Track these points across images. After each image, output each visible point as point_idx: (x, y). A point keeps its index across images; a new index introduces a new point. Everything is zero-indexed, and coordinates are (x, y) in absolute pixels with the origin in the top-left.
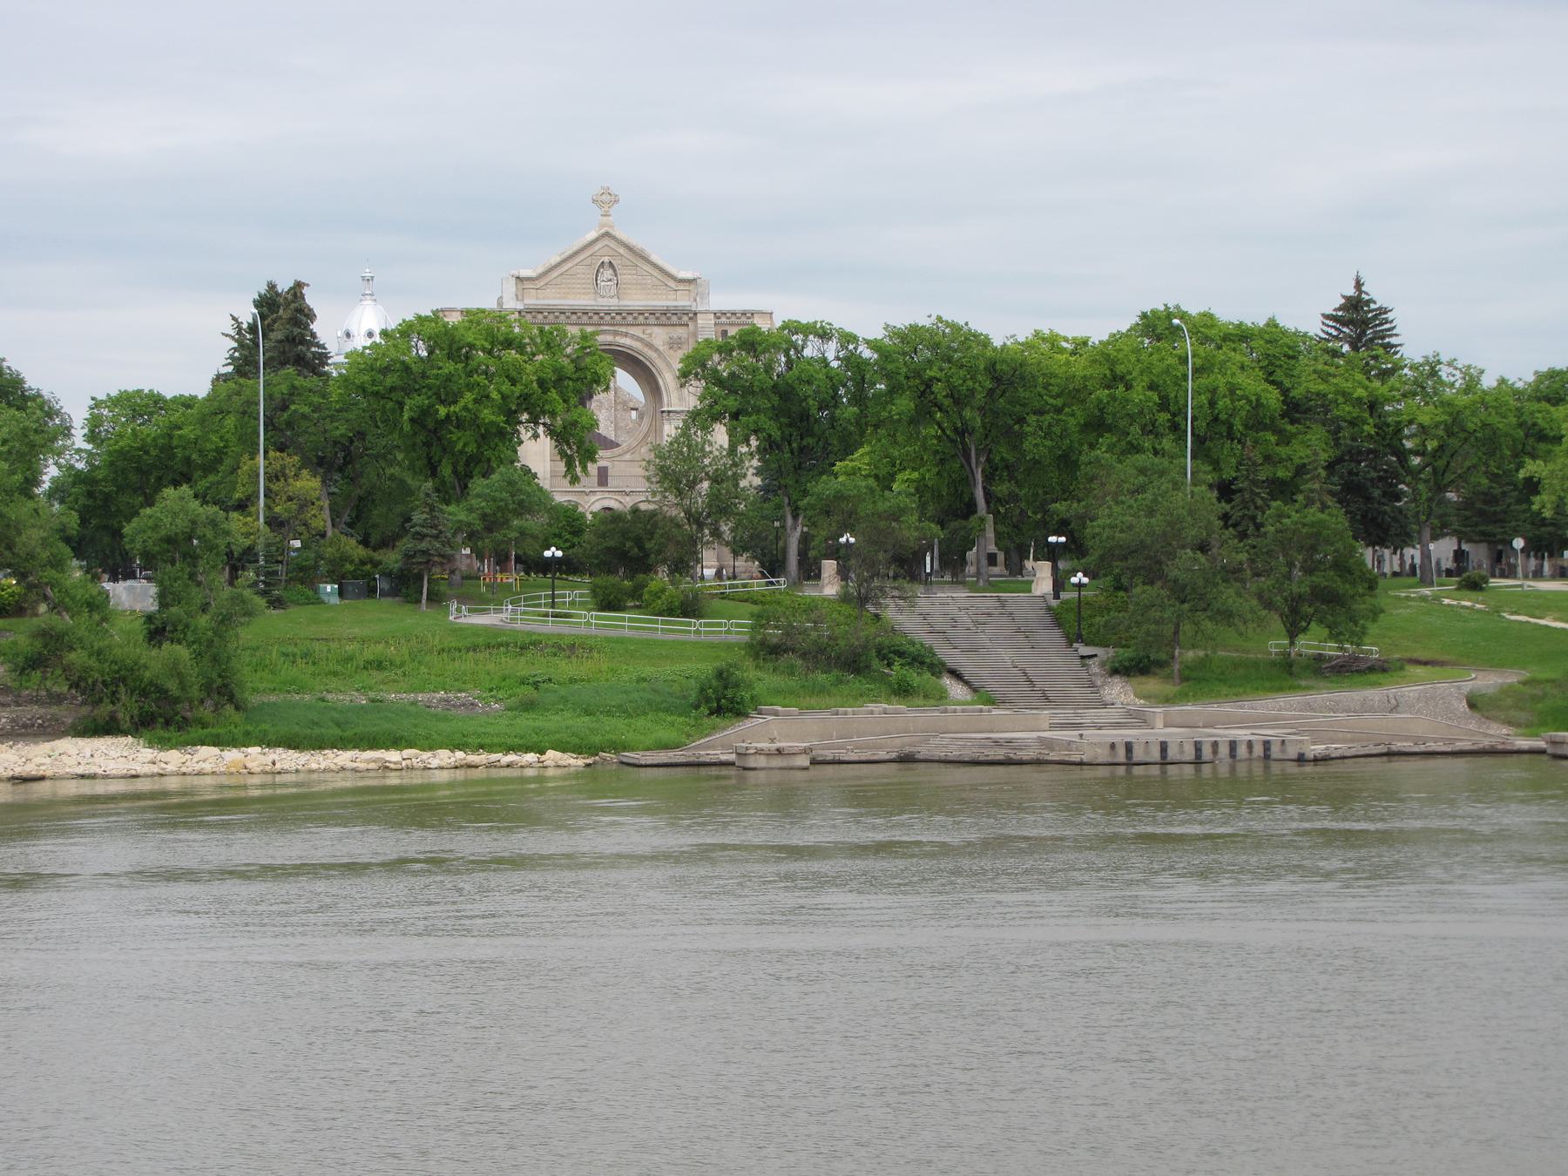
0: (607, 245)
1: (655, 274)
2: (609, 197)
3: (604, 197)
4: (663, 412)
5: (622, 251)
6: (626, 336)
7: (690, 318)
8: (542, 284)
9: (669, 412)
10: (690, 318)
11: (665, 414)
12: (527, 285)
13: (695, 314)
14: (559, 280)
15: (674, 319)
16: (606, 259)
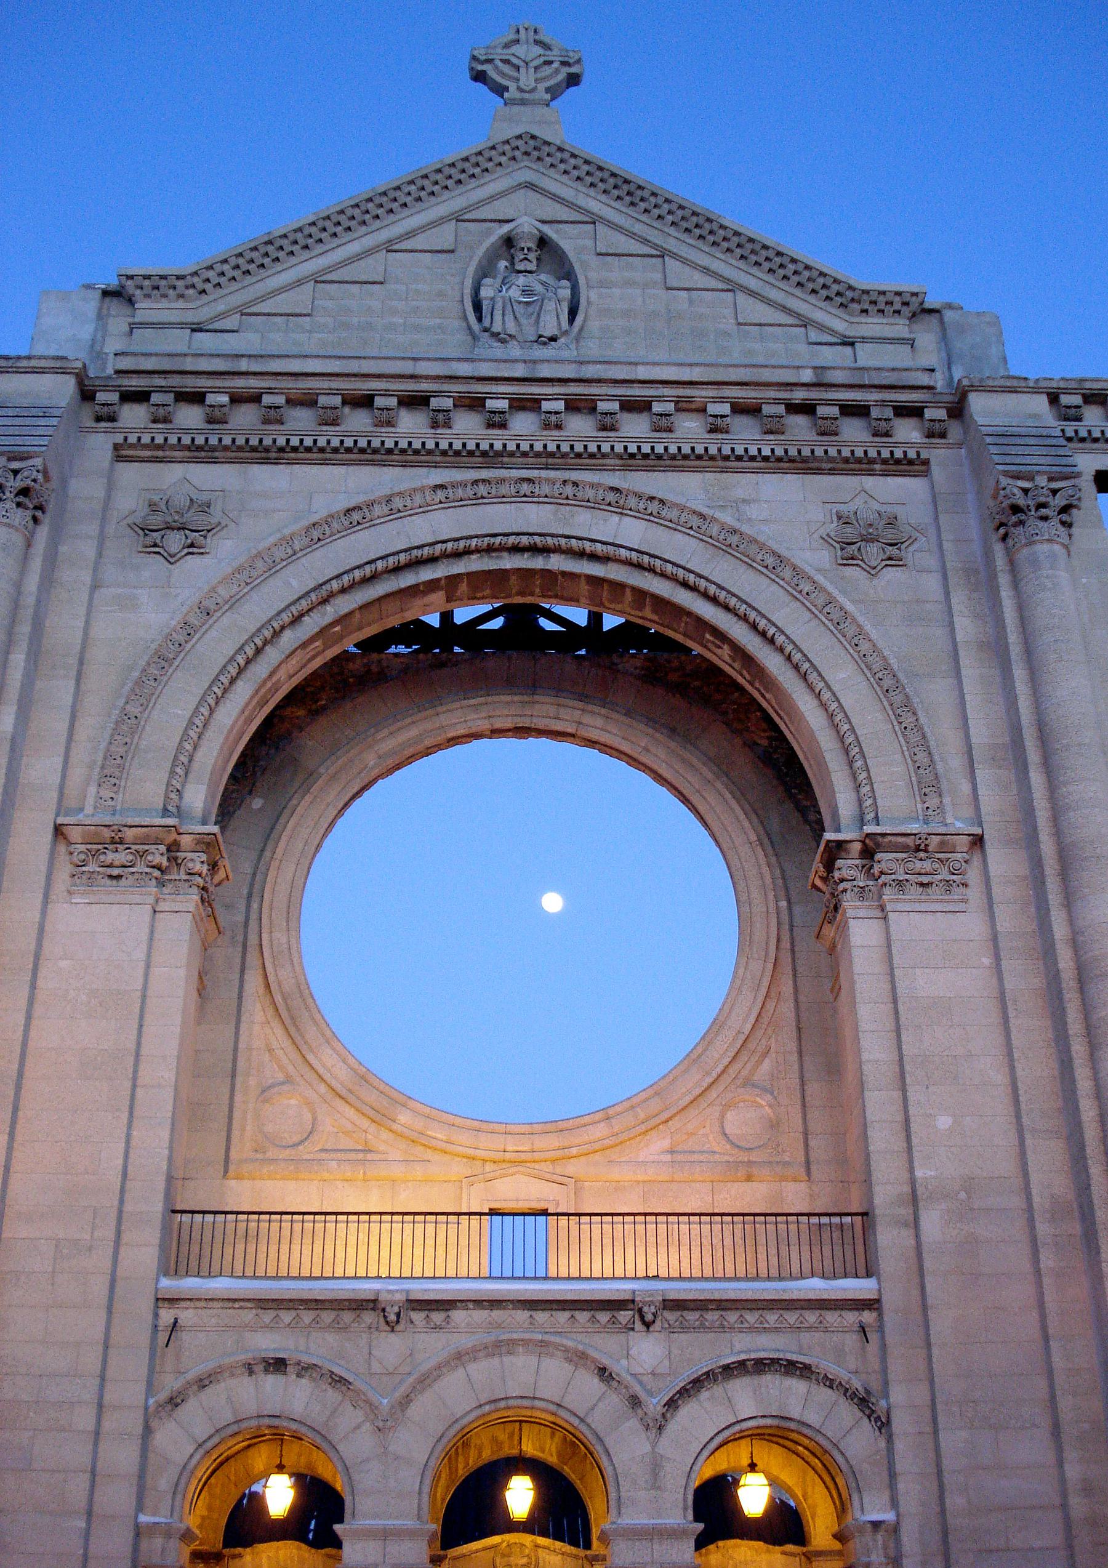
0: (519, 186)
1: (753, 284)
2: (538, 50)
3: (515, 49)
4: (836, 849)
5: (595, 204)
6: (621, 511)
7: (935, 433)
8: (221, 307)
9: (869, 850)
10: (935, 433)
11: (847, 866)
12: (148, 309)
13: (958, 410)
14: (298, 300)
15: (854, 432)
16: (527, 226)
